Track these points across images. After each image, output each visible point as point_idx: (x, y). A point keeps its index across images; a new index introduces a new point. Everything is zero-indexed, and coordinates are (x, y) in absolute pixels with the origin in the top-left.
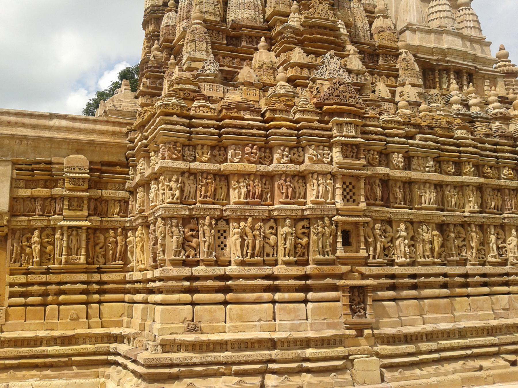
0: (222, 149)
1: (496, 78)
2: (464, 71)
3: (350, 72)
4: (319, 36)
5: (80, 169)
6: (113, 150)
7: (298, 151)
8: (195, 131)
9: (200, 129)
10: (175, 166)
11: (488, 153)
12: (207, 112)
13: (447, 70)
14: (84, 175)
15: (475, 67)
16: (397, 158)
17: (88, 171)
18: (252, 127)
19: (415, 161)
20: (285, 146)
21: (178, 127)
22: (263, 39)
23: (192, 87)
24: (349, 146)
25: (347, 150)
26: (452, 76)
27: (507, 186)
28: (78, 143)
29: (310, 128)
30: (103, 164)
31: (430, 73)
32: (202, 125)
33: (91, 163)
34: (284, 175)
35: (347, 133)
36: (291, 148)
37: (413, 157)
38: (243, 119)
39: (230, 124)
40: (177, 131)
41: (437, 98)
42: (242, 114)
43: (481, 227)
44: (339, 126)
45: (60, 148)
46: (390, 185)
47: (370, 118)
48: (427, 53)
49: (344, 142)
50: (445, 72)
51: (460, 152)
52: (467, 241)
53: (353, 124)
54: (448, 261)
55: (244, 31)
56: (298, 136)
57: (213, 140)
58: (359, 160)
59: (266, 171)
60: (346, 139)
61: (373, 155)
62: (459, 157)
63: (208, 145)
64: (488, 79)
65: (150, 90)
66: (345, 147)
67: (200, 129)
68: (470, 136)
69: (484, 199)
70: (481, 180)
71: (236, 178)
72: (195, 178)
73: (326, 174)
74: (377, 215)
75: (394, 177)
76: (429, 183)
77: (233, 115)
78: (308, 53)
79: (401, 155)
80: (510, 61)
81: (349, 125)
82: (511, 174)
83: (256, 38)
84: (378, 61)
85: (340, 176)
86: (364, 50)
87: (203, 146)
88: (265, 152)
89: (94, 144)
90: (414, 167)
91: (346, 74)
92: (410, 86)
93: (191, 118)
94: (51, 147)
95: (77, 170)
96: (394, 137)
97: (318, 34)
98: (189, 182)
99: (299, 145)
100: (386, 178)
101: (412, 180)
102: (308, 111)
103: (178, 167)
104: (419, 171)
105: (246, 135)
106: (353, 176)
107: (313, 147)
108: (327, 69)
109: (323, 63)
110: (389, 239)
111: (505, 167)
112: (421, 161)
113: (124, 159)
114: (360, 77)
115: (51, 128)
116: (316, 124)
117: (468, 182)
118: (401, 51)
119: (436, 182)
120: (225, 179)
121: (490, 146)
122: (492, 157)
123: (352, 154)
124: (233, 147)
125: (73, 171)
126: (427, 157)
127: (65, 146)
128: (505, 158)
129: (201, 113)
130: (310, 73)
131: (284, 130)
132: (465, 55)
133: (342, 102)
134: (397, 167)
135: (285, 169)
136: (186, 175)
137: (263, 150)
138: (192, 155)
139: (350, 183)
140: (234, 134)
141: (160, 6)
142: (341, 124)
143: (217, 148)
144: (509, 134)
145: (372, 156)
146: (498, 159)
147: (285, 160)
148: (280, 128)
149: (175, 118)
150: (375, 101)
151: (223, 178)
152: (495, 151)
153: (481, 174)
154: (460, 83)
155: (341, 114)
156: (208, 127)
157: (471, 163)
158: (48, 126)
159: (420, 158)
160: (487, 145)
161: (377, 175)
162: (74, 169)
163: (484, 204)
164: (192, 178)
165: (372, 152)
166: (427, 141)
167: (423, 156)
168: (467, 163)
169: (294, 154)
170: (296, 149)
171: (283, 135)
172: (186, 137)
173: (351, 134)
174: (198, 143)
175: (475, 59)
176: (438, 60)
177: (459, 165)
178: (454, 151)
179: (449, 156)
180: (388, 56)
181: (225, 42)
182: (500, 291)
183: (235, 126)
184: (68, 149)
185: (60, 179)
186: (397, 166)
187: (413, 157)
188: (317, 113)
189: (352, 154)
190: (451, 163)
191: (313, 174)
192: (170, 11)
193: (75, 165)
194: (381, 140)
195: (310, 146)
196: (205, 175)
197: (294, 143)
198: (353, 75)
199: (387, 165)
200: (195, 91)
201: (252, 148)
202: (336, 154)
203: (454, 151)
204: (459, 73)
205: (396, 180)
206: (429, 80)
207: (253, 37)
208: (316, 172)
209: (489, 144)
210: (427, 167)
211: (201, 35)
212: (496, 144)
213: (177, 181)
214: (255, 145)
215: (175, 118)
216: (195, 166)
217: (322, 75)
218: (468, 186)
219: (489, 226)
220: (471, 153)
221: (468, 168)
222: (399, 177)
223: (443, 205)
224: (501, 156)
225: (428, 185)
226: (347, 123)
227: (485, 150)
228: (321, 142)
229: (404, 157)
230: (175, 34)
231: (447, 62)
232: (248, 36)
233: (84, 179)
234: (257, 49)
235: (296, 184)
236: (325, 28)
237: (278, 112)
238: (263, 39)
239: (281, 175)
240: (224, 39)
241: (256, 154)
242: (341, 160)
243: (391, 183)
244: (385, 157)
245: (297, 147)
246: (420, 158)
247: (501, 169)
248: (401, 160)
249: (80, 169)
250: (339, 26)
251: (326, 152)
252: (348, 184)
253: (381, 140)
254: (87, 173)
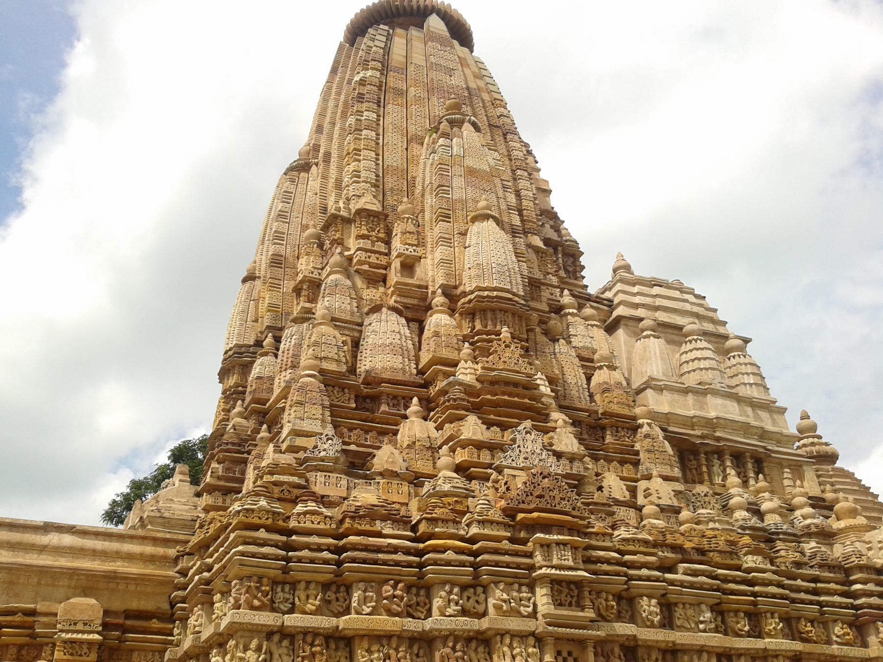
0: (342, 589)
1: (801, 466)
2: (748, 454)
3: (558, 455)
4: (506, 397)
5: (85, 624)
6: (149, 589)
7: (475, 594)
8: (297, 557)
9: (305, 553)
10: (256, 621)
11: (803, 596)
12: (319, 523)
13: (719, 453)
14: (91, 636)
15: (764, 448)
16: (649, 607)
17: (100, 628)
18: (395, 550)
19: (679, 612)
20: (453, 584)
21: (266, 550)
22: (415, 400)
23: (295, 479)
24: (564, 584)
25: (560, 592)
26: (728, 463)
27: (844, 657)
28: (88, 576)
29: (496, 552)
30: (129, 614)
31: (691, 457)
32: (307, 546)
33: (106, 613)
34: (451, 638)
35: (559, 562)
36: (464, 588)
37: (676, 604)
38: (379, 535)
39: (357, 544)
40: (265, 556)
41: (707, 499)
42: (378, 525)
44: (545, 548)
45: (53, 585)
46: (640, 655)
47: (597, 534)
48: (684, 426)
49: (555, 577)
50: (716, 456)
51: (755, 594)
53: (569, 546)
55: (385, 388)
56: (475, 566)
57: (326, 572)
58: (582, 610)
59: (420, 629)
60: (558, 572)
61: (606, 600)
62: (754, 604)
63: (317, 582)
64: (789, 467)
65: (222, 483)
66: (556, 587)
67: (305, 553)
68: (769, 566)
70: (798, 646)
71: (365, 645)
72: (292, 643)
73: (527, 636)
75: (646, 641)
76: (708, 652)
77: (363, 527)
78: (489, 424)
79: (654, 601)
80: (820, 437)
81: (562, 547)
82: (848, 634)
83: (404, 398)
84: (603, 438)
85: (550, 640)
86: (581, 419)
87: (308, 583)
88: (417, 595)
89: (115, 578)
90: (679, 623)
91: (552, 459)
92: (659, 480)
93: (290, 532)
94: (39, 583)
95: (80, 627)
96: (640, 568)
97: (504, 394)
98: (280, 651)
99: (477, 582)
100: (632, 644)
101: (678, 647)
102: (492, 522)
103: (262, 622)
104: (688, 630)
105: (385, 563)
106: (573, 640)
107: (502, 586)
108: (520, 451)
109: (514, 440)
111: (835, 621)
112: (690, 612)
113: (166, 606)
114: (576, 464)
115: (42, 549)
116: (506, 545)
117: (775, 651)
118: (640, 421)
119: (720, 651)
120: (346, 646)
121: (804, 584)
122: (811, 603)
123: (569, 599)
124: (361, 585)
125: (72, 628)
126: (699, 604)
127: (64, 582)
128: (833, 605)
129: (309, 525)
130: (493, 456)
131: (450, 555)
132: (746, 428)
133: (549, 506)
134: (649, 623)
135: (453, 626)
136: (276, 638)
137: (414, 590)
138: (288, 600)
139: (570, 653)
140: (364, 561)
141: (250, 346)
142: (548, 546)
143: (334, 588)
144: (834, 563)
145: (604, 603)
146: (822, 607)
147: (452, 609)
148: (444, 552)
149: (262, 534)
150: (604, 505)
151: (342, 644)
152: (815, 592)
153: (797, 635)
154: (743, 474)
155: (546, 527)
156: (319, 549)
157: (776, 615)
158: (39, 546)
159: (688, 606)
160: (799, 582)
161: (616, 638)
162: (75, 624)
164: (285, 643)
165: (604, 595)
166: (698, 576)
167: (693, 602)
168: (769, 615)
169: (469, 598)
170: (472, 590)
171: (448, 563)
172: (279, 567)
173: (566, 563)
174: (299, 578)
175: (763, 434)
176: (702, 437)
177: (755, 617)
178: (744, 593)
179: (737, 602)
180: (620, 429)
181: (354, 405)
183: (366, 548)
184: (69, 587)
185: (47, 644)
186: (648, 620)
187: (676, 604)
188: (506, 526)
190: (742, 615)
191: (502, 635)
192: (265, 354)
193: (78, 617)
194: (617, 574)
195: (496, 583)
196: (309, 639)
197: (468, 579)
198: (564, 461)
199: (632, 620)
200: (299, 486)
201: (395, 587)
202: (542, 598)
203: (744, 593)
204: (738, 458)
205: (650, 647)
206: (690, 470)
207: (400, 398)
208: (507, 632)
209: (803, 580)
210: (702, 622)
211: (314, 394)
212: (815, 580)
213: (259, 649)
214: (400, 581)
215: (262, 534)
216: (293, 620)
217: (513, 460)
218: (777, 656)
220: (774, 596)
221: (772, 624)
222: (654, 641)
224: (827, 602)
226: (558, 543)
227: (798, 590)
228: (515, 576)
229: (660, 604)
230: (271, 390)
231: (718, 439)
232: (391, 396)
233: (90, 643)
234: (405, 417)
235: (473, 655)
236: (516, 384)
237: (440, 523)
238: (415, 400)
239: (445, 638)
240: (353, 401)
241: (402, 598)
242: (551, 609)
243: (641, 652)
245: (474, 586)
246: (688, 606)
247: (830, 624)
248: (655, 609)
249: (85, 624)
250: (538, 382)
251: (525, 595)
252: (565, 654)
253: (617, 574)
254: (98, 633)
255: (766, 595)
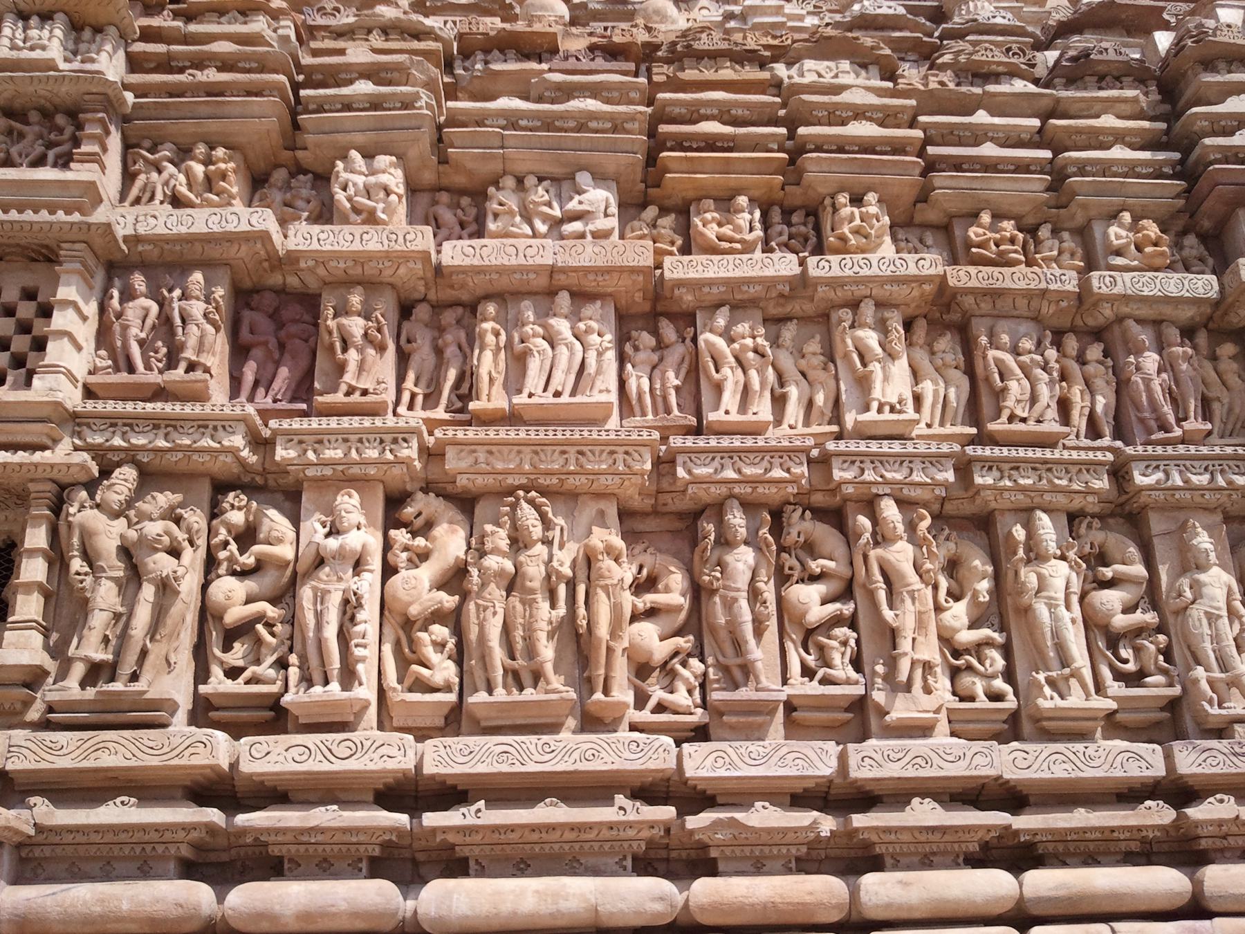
11: (989, 150)
24: (34, 116)
35: (15, 54)
43: (969, 521)
52: (858, 592)
54: (716, 711)
61: (207, 162)
69: (980, 370)
74: (161, 443)
81: (34, 21)
110: (268, 581)
157: (871, 197)
160: (981, 117)
163: (986, 401)
165: (201, 149)
168: (843, 198)
179: (727, 167)
182: (1114, 896)
186: (357, 210)
189: (39, 149)
219: (1026, 514)
220: (868, 146)
223: (699, 415)
225: (564, 299)
227: (978, 136)
244: (292, 171)
246: (530, 181)
247: (1097, 229)
255: (841, 146)
